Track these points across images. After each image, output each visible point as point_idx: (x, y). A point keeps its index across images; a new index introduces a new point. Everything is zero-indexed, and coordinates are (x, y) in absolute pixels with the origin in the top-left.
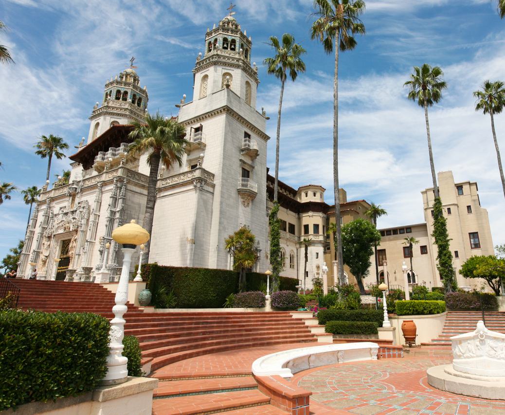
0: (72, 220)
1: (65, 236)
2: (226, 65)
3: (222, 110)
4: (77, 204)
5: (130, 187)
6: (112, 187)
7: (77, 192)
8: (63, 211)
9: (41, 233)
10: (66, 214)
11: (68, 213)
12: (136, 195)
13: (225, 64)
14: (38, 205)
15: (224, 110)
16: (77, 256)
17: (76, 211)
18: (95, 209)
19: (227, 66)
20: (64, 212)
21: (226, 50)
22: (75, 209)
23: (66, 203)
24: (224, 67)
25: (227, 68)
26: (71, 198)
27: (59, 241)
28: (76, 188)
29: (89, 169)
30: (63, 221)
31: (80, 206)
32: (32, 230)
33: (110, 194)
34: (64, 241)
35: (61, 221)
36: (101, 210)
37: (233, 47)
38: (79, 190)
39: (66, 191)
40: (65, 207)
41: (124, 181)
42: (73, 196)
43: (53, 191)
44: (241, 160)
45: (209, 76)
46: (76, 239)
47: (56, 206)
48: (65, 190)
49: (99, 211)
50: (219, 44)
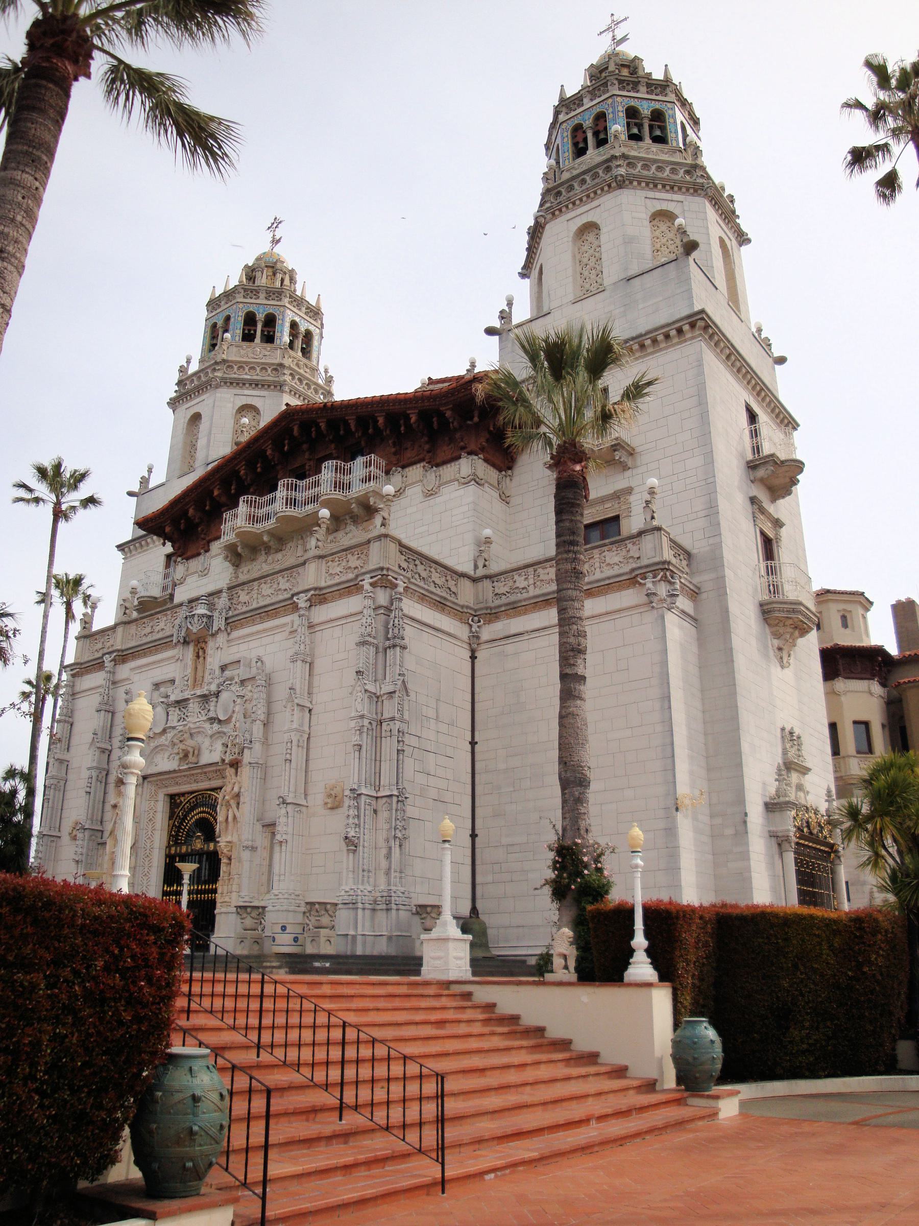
0: (207, 725)
1: (179, 780)
2: (655, 186)
3: (686, 328)
4: (218, 672)
5: (411, 607)
6: (353, 603)
7: (215, 628)
8: (167, 696)
9: (97, 768)
10: (181, 703)
11: (188, 699)
12: (427, 637)
13: (653, 184)
14: (73, 676)
15: (693, 325)
16: (246, 855)
17: (217, 695)
18: (298, 687)
19: (660, 191)
20: (173, 698)
21: (640, 144)
22: (213, 688)
23: (173, 665)
24: (651, 194)
25: (658, 195)
26: (190, 651)
27: (161, 797)
28: (210, 617)
29: (199, 554)
30: (174, 728)
31: (232, 679)
32: (61, 757)
33: (352, 633)
35: (164, 731)
36: (315, 690)
37: (658, 133)
38: (218, 623)
39: (164, 626)
40: (173, 681)
41: (396, 586)
42: (197, 642)
43: (120, 630)
44: (753, 500)
45: (604, 230)
46: (238, 795)
47: (136, 678)
48: (162, 625)
49: (310, 694)
50: (617, 127)
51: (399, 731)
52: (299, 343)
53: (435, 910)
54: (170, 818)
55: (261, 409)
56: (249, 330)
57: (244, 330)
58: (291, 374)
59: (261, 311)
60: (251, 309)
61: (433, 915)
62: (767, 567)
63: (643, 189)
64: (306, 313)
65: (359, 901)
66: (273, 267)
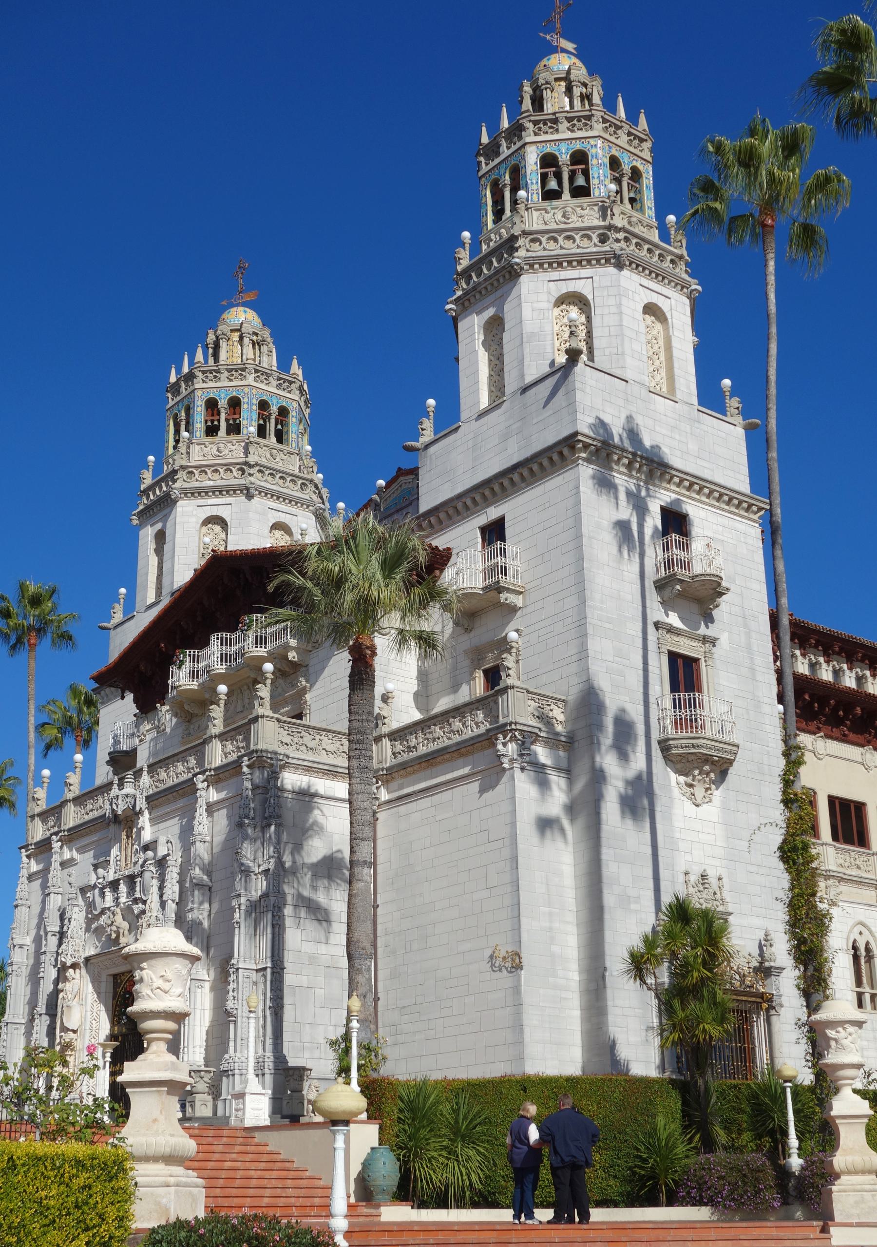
13: (556, 262)
24: (555, 275)
25: (564, 274)
27: (104, 978)
34: (115, 976)
51: (274, 907)
52: (271, 427)
53: (297, 1072)
54: (114, 998)
55: (228, 520)
56: (212, 421)
57: (206, 421)
58: (260, 471)
59: (223, 395)
60: (212, 395)
61: (295, 1077)
62: (674, 700)
63: (545, 270)
64: (279, 386)
65: (236, 1067)
66: (239, 330)
